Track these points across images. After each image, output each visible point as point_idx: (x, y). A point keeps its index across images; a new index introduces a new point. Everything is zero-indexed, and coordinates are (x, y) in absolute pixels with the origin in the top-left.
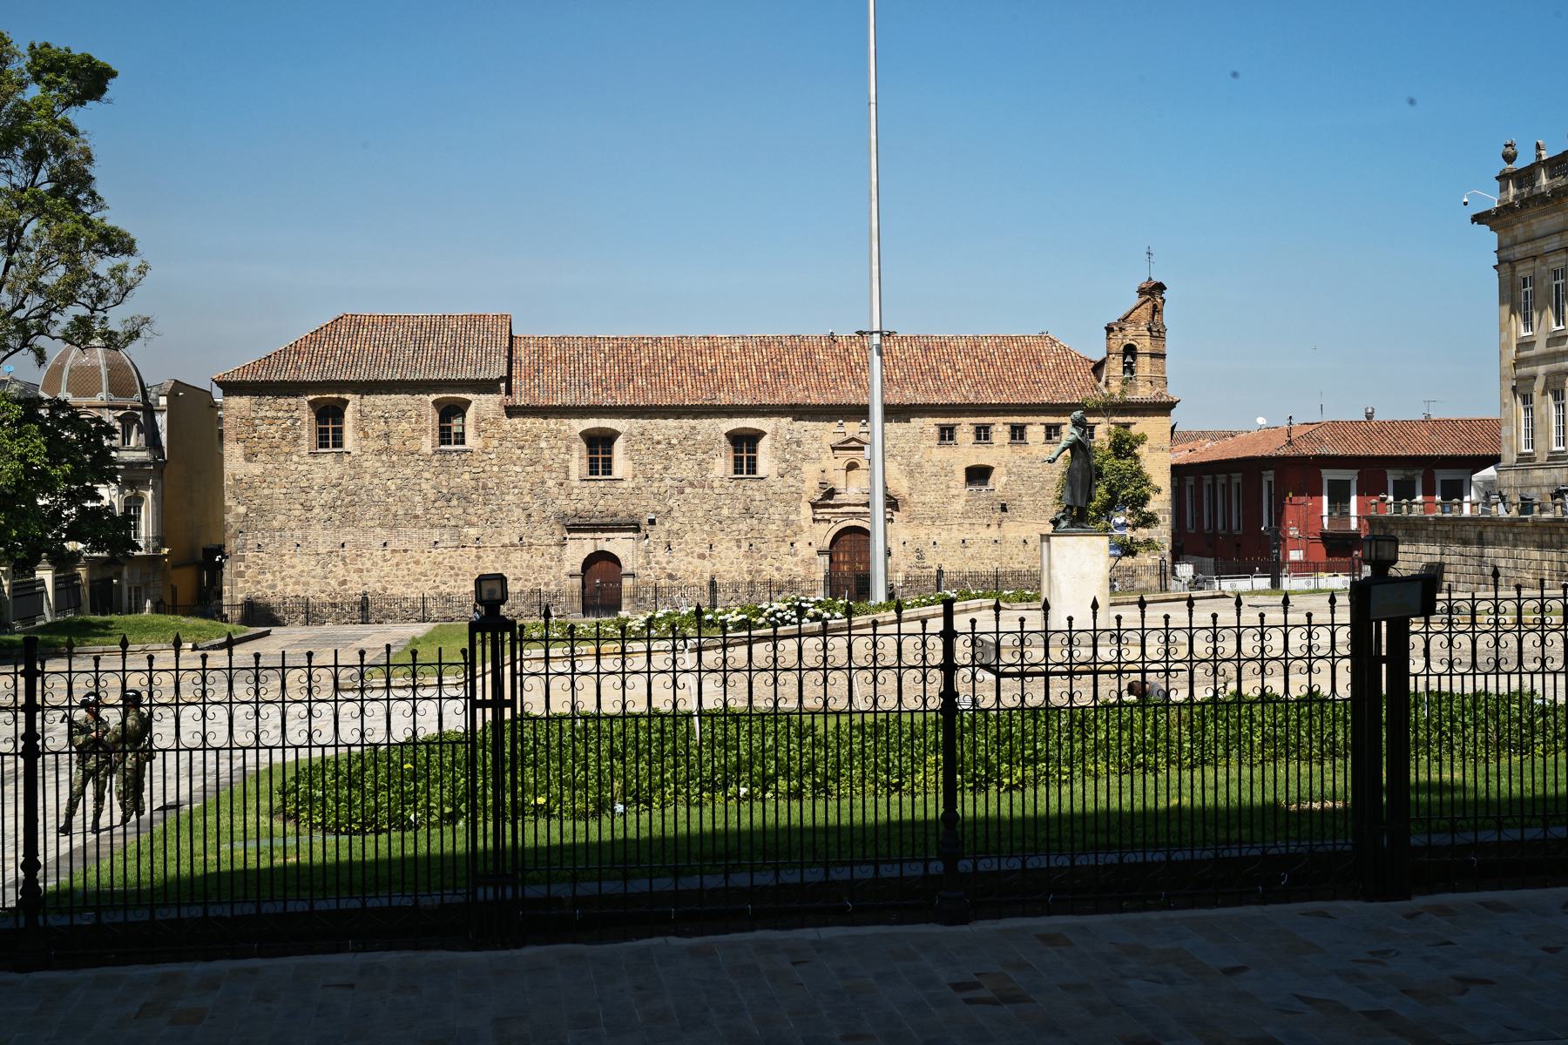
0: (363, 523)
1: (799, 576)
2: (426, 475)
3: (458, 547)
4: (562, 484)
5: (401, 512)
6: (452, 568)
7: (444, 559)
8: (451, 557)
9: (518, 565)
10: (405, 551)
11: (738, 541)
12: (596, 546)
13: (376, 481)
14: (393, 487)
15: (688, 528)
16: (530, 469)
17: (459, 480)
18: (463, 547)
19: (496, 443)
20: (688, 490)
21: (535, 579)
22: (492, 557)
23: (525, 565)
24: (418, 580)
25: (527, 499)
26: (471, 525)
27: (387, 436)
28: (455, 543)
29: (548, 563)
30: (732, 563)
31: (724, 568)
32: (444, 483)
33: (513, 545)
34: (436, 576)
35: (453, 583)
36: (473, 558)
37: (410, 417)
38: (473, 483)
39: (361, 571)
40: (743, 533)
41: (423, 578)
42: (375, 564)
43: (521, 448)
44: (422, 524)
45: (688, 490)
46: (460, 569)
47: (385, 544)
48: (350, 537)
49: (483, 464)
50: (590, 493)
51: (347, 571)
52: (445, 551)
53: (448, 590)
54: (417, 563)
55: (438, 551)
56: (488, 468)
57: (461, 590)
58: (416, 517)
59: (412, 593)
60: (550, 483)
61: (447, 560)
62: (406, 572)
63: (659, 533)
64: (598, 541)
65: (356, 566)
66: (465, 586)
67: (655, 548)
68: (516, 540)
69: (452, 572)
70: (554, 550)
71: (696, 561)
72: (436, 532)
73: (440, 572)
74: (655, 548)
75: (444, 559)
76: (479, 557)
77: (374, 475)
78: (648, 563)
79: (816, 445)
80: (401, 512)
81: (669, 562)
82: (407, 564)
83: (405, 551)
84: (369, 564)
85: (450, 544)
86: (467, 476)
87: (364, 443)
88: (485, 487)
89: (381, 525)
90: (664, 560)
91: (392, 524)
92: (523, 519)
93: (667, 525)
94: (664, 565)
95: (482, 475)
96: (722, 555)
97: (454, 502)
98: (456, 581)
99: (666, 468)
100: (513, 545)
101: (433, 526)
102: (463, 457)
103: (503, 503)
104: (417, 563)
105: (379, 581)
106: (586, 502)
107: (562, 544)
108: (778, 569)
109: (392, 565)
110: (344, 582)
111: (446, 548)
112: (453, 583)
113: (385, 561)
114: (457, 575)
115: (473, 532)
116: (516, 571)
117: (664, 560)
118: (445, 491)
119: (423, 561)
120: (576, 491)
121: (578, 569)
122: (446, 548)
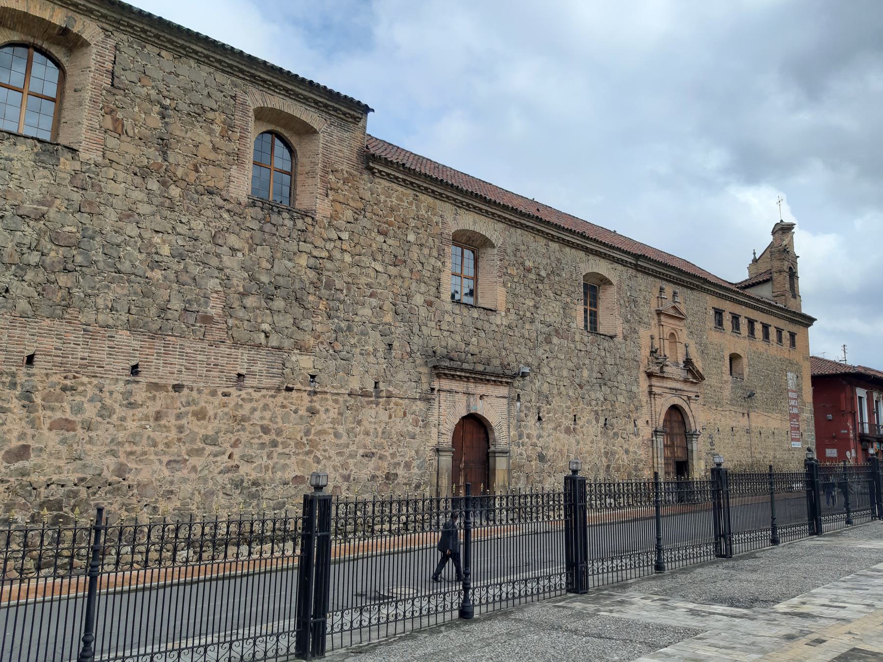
0: (89, 316)
1: (641, 461)
2: (233, 240)
3: (278, 390)
4: (430, 304)
5: (176, 304)
6: (266, 430)
8: (266, 407)
9: (371, 428)
10: (177, 388)
11: (596, 413)
12: (468, 406)
13: (131, 229)
14: (166, 250)
15: (555, 391)
16: (393, 270)
17: (290, 264)
18: (289, 389)
19: (349, 214)
20: (555, 340)
21: (393, 455)
22: (333, 414)
23: (380, 430)
24: (199, 452)
25: (388, 318)
26: (302, 349)
27: (164, 145)
28: (276, 381)
29: (410, 428)
30: (592, 442)
31: (587, 448)
32: (265, 264)
33: (365, 394)
34: (235, 445)
35: (265, 461)
36: (303, 412)
37: (212, 122)
38: (312, 274)
39: (66, 425)
40: (599, 403)
41: (209, 449)
42: (105, 412)
43: (385, 234)
44: (217, 335)
45: (555, 340)
46: (279, 432)
47: (135, 370)
48: (49, 343)
49: (329, 246)
50: (463, 325)
51: (33, 423)
52: (256, 395)
53: (254, 475)
54: (201, 415)
55: (243, 393)
56: (337, 254)
57: (279, 474)
58: (207, 319)
59: (185, 480)
60: (419, 299)
61: (257, 414)
62: (173, 434)
63: (530, 389)
64: (472, 399)
65: (58, 415)
66: (285, 467)
67: (526, 416)
68: (370, 388)
69: (266, 438)
70: (420, 405)
71: (562, 436)
72: (243, 355)
73: (244, 436)
74: (526, 416)
75: (254, 410)
76: (313, 412)
77: (129, 215)
78: (520, 436)
79: (647, 309)
80: (176, 304)
81: (539, 437)
82: (179, 417)
83: (177, 388)
84: (90, 411)
85: (267, 382)
86: (303, 260)
87: (112, 142)
88: (329, 286)
89: (131, 327)
90: (535, 433)
91: (155, 327)
92: (382, 347)
93: (538, 384)
94: (535, 440)
95: (328, 265)
96: (584, 430)
97: (279, 304)
98: (270, 456)
99: (536, 307)
100: (365, 394)
101: (237, 344)
102: (300, 224)
103: (357, 319)
104: (201, 415)
105: (113, 453)
106: (458, 338)
107: (427, 398)
108: (627, 452)
109: (147, 418)
110: (23, 452)
111: (258, 389)
112: (265, 461)
113: (131, 405)
114: (274, 444)
115: (306, 362)
116: (368, 441)
117: (535, 433)
118: (265, 279)
119: (211, 413)
120: (448, 318)
121: (447, 440)
122: (258, 389)
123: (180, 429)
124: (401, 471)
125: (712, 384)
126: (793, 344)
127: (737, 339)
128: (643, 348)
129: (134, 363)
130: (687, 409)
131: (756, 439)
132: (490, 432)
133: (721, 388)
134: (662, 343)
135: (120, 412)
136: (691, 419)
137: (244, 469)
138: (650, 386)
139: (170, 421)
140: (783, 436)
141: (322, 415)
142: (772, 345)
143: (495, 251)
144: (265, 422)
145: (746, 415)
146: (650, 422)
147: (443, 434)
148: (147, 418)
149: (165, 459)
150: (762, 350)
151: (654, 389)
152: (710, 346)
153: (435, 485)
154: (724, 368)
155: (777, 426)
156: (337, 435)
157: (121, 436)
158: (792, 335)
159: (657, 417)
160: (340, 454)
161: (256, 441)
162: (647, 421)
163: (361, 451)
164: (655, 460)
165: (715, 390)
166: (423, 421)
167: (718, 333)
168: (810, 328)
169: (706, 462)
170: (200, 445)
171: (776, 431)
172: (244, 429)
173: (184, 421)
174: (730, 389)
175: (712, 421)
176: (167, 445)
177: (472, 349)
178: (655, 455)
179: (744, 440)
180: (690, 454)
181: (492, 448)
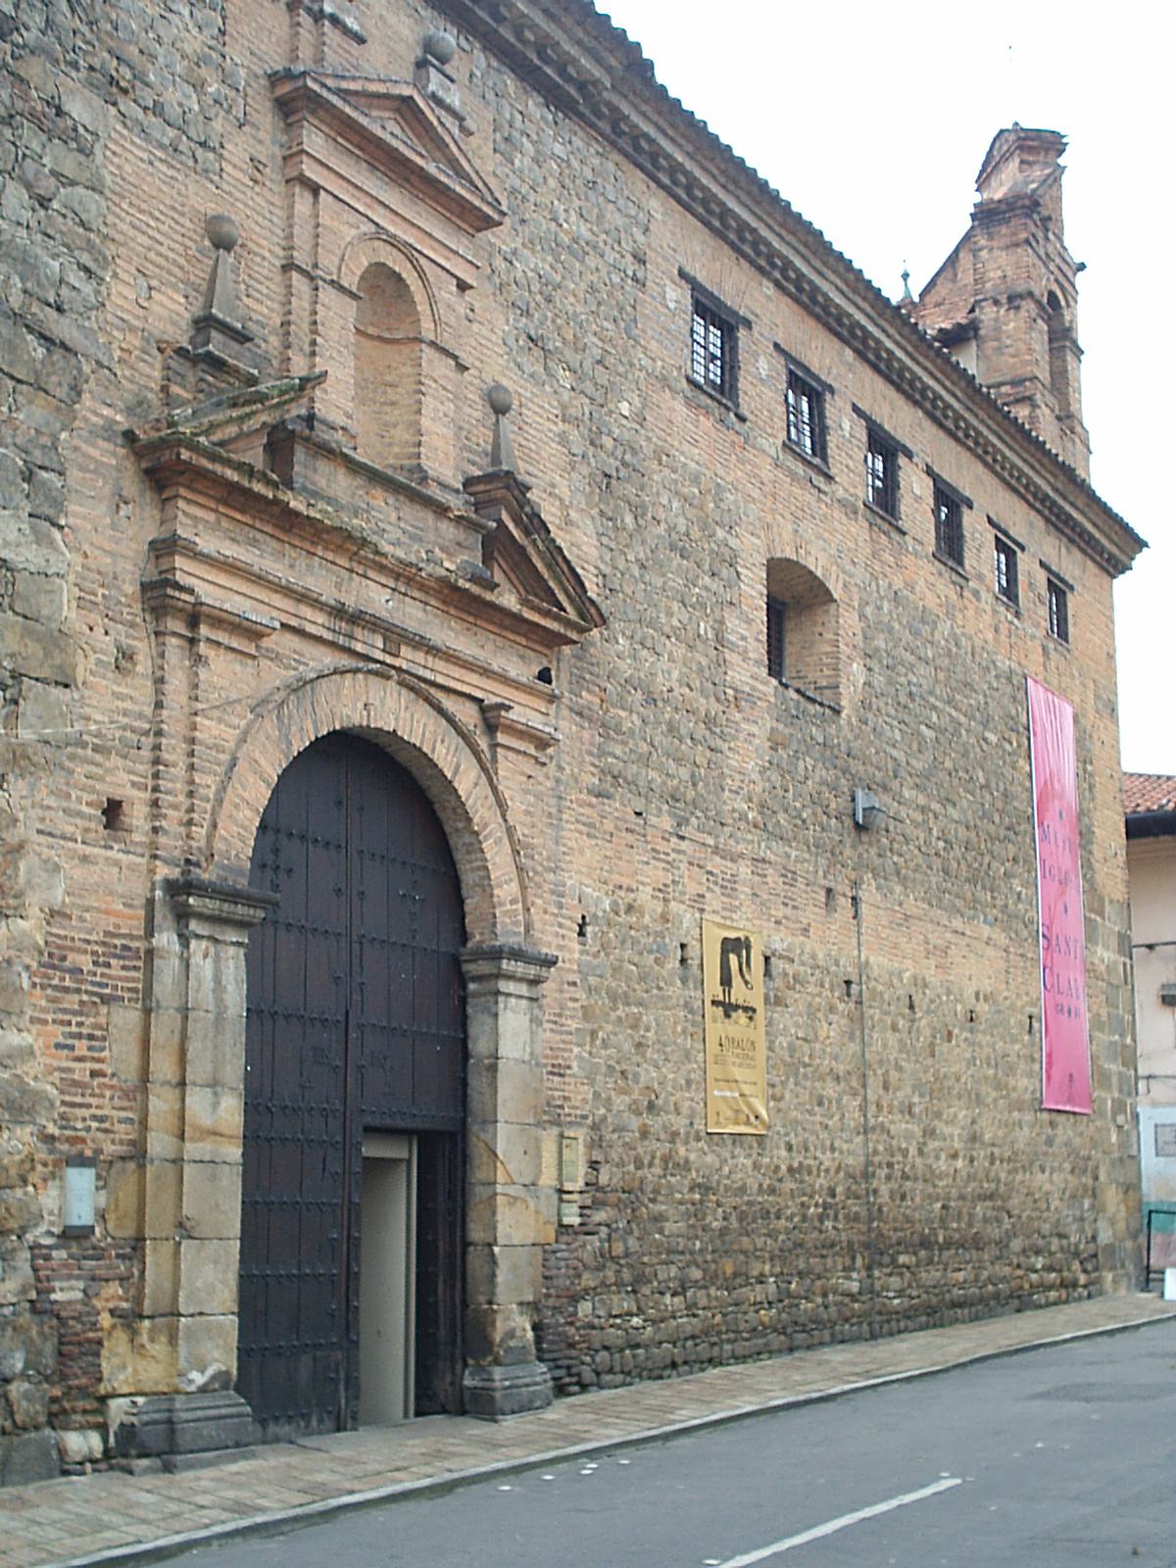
125: (661, 684)
127: (808, 497)
128: (126, 269)
130: (467, 782)
131: (892, 1039)
133: (709, 722)
134: (301, 305)
136: (497, 856)
138: (165, 547)
140: (1014, 1041)
142: (976, 594)
145: (844, 903)
146: (137, 815)
150: (931, 602)
151: (185, 569)
152: (658, 475)
154: (732, 622)
155: (987, 986)
158: (1058, 589)
159: (207, 783)
162: (113, 811)
164: (160, 1104)
165: (672, 729)
167: (706, 423)
168: (1120, 583)
169: (596, 1143)
171: (982, 1008)
174: (761, 741)
175: (644, 896)
178: (163, 1066)
179: (832, 1031)
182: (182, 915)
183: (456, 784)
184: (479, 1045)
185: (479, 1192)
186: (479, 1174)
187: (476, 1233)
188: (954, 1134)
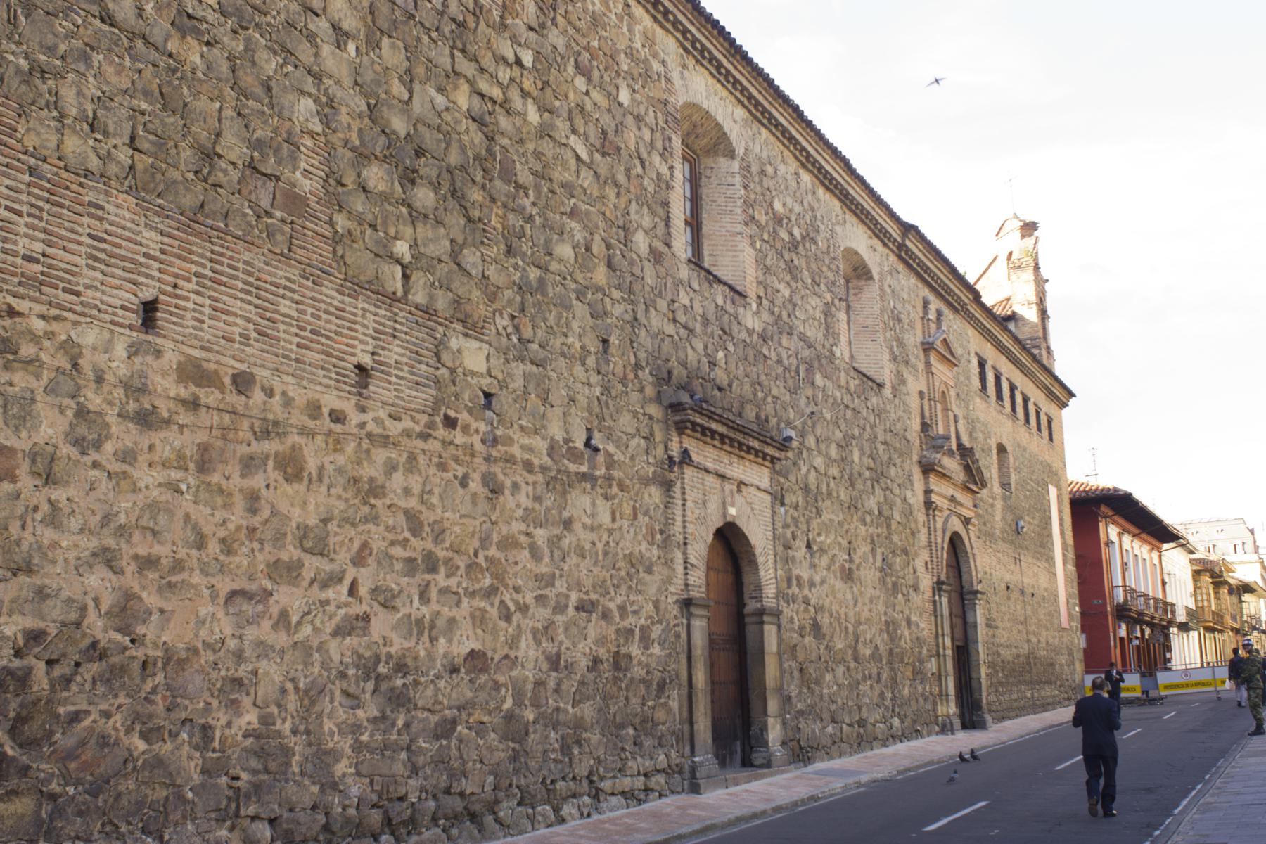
5: (234, 148)
7: (391, 468)
17: (440, 100)
24: (287, 572)
33: (574, 455)
34: (358, 561)
41: (312, 564)
53: (398, 645)
54: (291, 467)
61: (398, 479)
62: (237, 517)
70: (654, 495)
75: (391, 468)
82: (249, 465)
83: (242, 382)
86: (463, 98)
88: (508, 174)
92: (594, 346)
97: (424, 197)
105: (108, 558)
109: (180, 462)
114: (431, 565)
118: (399, 125)
119: (312, 465)
123: (253, 499)
124: (635, 650)
126: (1051, 439)
129: (147, 295)
132: (746, 569)
135: (123, 435)
137: (381, 624)
139: (230, 476)
141: (507, 499)
143: (736, 165)
144: (413, 503)
147: (693, 565)
148: (180, 462)
149: (225, 586)
151: (934, 498)
153: (685, 684)
156: (535, 554)
157: (125, 507)
160: (540, 599)
161: (397, 551)
163: (574, 597)
166: (662, 532)
168: (1065, 411)
170: (290, 552)
172: (375, 519)
173: (257, 481)
176: (228, 547)
177: (720, 375)
180: (970, 632)
181: (751, 606)
182: (940, 590)
183: (1169, 600)
184: (970, 619)
185: (973, 663)
186: (973, 658)
187: (974, 675)
188: (1043, 640)
